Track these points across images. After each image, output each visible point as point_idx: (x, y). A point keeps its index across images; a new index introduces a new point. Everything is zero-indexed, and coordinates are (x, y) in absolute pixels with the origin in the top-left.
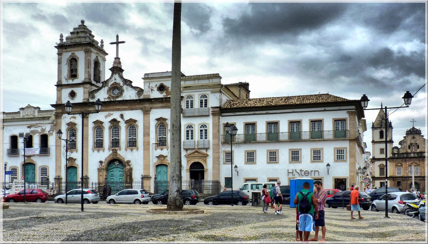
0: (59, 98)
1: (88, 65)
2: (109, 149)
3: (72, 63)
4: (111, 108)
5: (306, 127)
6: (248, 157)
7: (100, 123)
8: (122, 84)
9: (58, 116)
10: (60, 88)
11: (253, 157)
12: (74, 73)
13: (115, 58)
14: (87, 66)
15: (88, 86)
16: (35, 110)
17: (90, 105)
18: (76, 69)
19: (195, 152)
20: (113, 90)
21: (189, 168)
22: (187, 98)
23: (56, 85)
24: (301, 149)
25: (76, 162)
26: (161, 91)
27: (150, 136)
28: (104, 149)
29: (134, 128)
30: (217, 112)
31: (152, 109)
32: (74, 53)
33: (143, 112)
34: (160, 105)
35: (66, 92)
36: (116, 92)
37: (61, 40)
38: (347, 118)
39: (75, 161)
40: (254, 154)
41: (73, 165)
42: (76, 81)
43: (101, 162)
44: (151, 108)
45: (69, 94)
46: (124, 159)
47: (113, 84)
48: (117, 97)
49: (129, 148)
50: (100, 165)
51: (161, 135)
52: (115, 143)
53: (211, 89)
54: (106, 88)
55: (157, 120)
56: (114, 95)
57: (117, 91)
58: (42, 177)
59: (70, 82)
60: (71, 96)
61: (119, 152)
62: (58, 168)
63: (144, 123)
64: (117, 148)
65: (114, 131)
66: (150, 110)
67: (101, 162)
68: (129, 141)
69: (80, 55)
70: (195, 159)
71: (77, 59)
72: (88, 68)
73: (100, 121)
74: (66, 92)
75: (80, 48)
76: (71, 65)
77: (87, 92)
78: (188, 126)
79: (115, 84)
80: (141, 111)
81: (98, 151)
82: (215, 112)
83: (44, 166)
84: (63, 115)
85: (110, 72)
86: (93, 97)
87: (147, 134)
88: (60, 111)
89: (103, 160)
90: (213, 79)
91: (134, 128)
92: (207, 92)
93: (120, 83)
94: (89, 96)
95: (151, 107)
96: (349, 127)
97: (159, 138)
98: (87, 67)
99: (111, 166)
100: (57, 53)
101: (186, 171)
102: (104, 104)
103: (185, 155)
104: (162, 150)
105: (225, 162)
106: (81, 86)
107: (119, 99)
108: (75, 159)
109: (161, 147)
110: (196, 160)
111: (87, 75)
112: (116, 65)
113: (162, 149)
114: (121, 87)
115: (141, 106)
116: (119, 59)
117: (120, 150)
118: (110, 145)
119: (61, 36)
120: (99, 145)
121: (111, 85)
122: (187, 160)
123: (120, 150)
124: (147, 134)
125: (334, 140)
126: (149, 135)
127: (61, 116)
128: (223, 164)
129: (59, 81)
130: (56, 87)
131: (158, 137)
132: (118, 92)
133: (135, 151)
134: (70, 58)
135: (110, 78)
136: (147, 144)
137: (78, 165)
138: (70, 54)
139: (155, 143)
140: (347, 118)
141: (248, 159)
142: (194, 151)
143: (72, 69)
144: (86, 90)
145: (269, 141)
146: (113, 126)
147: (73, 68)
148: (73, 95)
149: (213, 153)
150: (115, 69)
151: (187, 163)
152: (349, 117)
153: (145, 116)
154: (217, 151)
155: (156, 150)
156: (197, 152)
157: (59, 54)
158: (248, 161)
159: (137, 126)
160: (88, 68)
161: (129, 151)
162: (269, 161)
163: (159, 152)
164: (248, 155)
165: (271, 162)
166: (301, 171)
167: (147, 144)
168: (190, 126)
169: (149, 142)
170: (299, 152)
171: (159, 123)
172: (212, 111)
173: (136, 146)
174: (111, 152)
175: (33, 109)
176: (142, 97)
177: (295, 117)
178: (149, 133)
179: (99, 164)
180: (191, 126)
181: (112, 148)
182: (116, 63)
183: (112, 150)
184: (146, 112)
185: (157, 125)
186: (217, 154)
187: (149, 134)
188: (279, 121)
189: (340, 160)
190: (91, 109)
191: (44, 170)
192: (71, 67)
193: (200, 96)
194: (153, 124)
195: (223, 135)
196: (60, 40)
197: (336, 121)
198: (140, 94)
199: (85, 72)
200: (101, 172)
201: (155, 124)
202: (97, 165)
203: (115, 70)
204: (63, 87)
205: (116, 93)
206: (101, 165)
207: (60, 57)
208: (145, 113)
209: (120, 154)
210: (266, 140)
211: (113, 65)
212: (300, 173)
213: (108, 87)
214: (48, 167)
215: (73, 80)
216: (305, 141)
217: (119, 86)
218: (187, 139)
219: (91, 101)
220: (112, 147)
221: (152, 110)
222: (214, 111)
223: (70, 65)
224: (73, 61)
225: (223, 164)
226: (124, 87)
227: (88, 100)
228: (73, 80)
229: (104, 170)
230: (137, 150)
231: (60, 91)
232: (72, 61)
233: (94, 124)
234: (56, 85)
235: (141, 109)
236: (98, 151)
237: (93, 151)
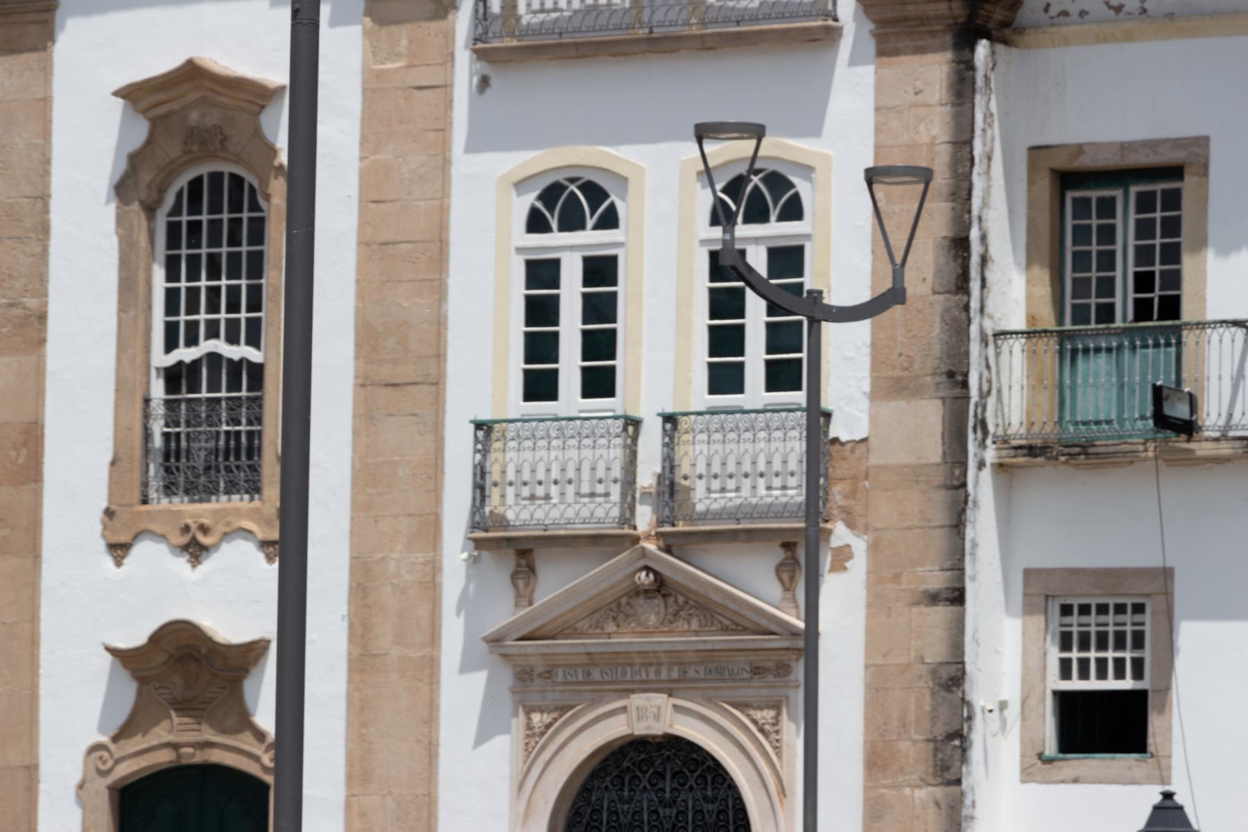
27: (42, 342)
51: (192, 327)
103: (495, 641)
104: (196, 560)
113: (195, 550)
128: (1027, 775)
131: (161, 359)
149: (877, 603)
156: (661, 587)
178: (31, 302)
180: (595, 193)
185: (146, 177)
186: (941, 613)
187: (42, 318)
195: (1029, 334)
218: (529, 395)
225: (1027, 775)
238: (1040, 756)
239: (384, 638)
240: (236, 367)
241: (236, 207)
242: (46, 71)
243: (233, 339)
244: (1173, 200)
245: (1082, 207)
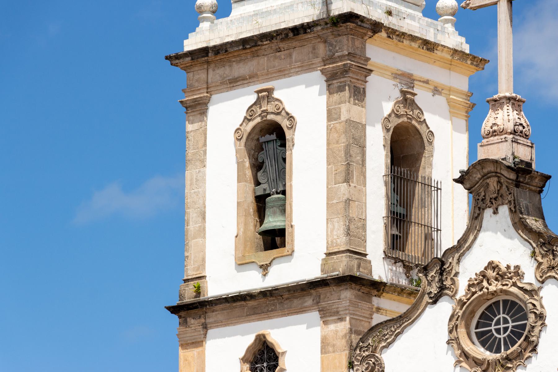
3: (262, 156)
20: (485, 319)
45: (244, 360)
56: (490, 349)
57: (506, 321)
71: (285, 124)
72: (347, 180)
77: (342, 343)
79: (491, 273)
93: (523, 269)
98: (341, 177)
106: (309, 301)
114: (532, 293)
130: (175, 318)
134: (252, 124)
143: (260, 192)
150: (485, 176)
192: (258, 183)
204: (212, 317)
205: (502, 336)
213: (452, 297)
215: (265, 268)
217: (514, 290)
223: (249, 173)
226: (542, 293)
231: (200, 349)
232: (263, 139)
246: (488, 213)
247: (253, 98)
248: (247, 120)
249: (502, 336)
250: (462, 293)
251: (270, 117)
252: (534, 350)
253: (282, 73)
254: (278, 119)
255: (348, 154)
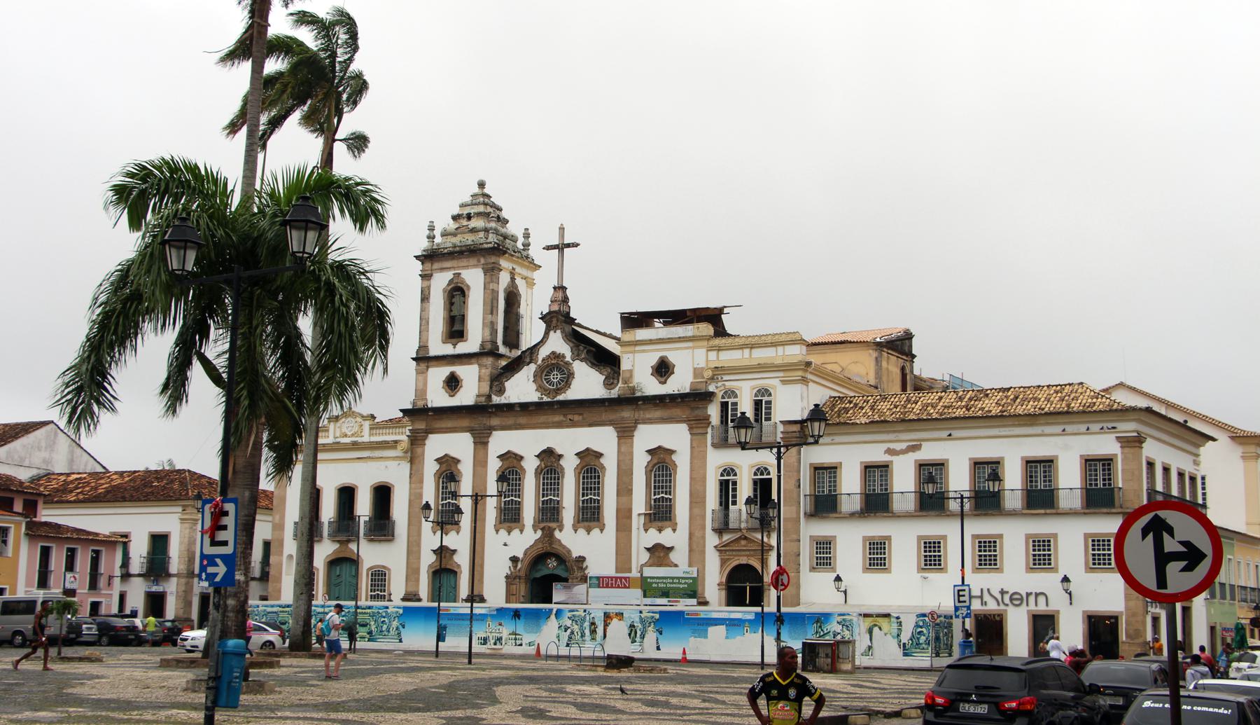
0: (421, 392)
1: (491, 308)
2: (535, 528)
3: (454, 300)
4: (542, 419)
5: (1013, 479)
6: (870, 554)
7: (515, 458)
8: (568, 358)
9: (417, 440)
10: (423, 366)
11: (885, 553)
12: (456, 328)
13: (555, 288)
14: (489, 308)
15: (489, 361)
16: (363, 423)
17: (492, 413)
18: (464, 316)
19: (740, 538)
20: (548, 374)
21: (724, 580)
22: (723, 397)
23: (413, 359)
24: (1001, 536)
25: (456, 558)
26: (661, 376)
28: (524, 525)
29: (595, 473)
30: (794, 434)
31: (640, 423)
32: (460, 274)
33: (618, 432)
34: (658, 413)
35: (439, 374)
36: (556, 377)
37: (431, 238)
38: (1116, 455)
39: (453, 554)
40: (886, 546)
41: (448, 567)
42: (463, 348)
43: (514, 560)
44: (637, 422)
46: (569, 551)
47: (549, 356)
48: (558, 391)
49: (582, 524)
50: (512, 568)
52: (549, 513)
53: (781, 374)
54: (533, 367)
55: (649, 452)
58: (373, 593)
59: (448, 349)
60: (448, 386)
61: (557, 534)
62: (412, 572)
63: (618, 460)
64: (553, 525)
65: (547, 479)
66: (636, 427)
67: (514, 560)
68: (583, 507)
69: (474, 277)
70: (741, 558)
71: (465, 288)
72: (492, 313)
73: (516, 455)
74: (439, 374)
75: (473, 261)
76: (452, 304)
77: (488, 378)
78: (725, 470)
79: (552, 356)
80: (468, 434)
81: (509, 533)
82: (789, 435)
83: (378, 566)
84: (430, 435)
85: (542, 326)
86: (501, 391)
87: (624, 489)
88: (421, 425)
89: (520, 556)
90: (786, 347)
91: (595, 473)
92: (772, 382)
94: (491, 388)
95: (636, 420)
96: (1122, 479)
97: (583, 501)
98: (489, 312)
99: (537, 571)
100: (420, 273)
101: (717, 587)
102: (525, 407)
105: (815, 566)
106: (473, 360)
107: (561, 397)
108: (454, 551)
109: (660, 524)
110: (743, 561)
111: (487, 332)
112: (555, 308)
113: (660, 530)
114: (568, 364)
115: (612, 416)
116: (563, 289)
117: (561, 531)
118: (537, 517)
119: (432, 228)
120: (510, 516)
121: (543, 360)
122: (722, 559)
123: (561, 531)
124: (624, 489)
125: (1085, 514)
126: (630, 492)
127: (425, 438)
128: (810, 571)
129: (423, 347)
131: (653, 497)
132: (559, 376)
133: (596, 531)
134: (450, 287)
135: (541, 341)
136: (624, 515)
137: (459, 566)
138: (449, 275)
139: (645, 514)
140: (1116, 455)
141: (870, 559)
142: (738, 535)
143: (452, 314)
144: (483, 371)
145: (920, 513)
146: (546, 467)
147: (455, 313)
148: (453, 383)
150: (552, 318)
151: (721, 566)
152: (1122, 453)
153: (622, 441)
154: (795, 537)
155: (646, 530)
156: (746, 538)
157: (426, 277)
158: (870, 565)
159: (603, 468)
160: (492, 313)
161: (582, 532)
162: (923, 566)
163: (653, 537)
164: (870, 549)
165: (928, 567)
166: (1003, 592)
167: (624, 515)
168: (729, 471)
169: (630, 510)
170: (998, 544)
171: (655, 461)
172: (782, 432)
173: (598, 520)
174: (539, 533)
175: (359, 419)
176: (614, 393)
177: (986, 449)
179: (510, 563)
180: (733, 470)
181: (542, 525)
182: (556, 301)
183: (543, 529)
184: (625, 433)
185: (651, 466)
187: (632, 490)
188: (947, 460)
189: (1102, 566)
190: (495, 421)
191: (380, 577)
192: (451, 311)
193: (755, 391)
194: (641, 461)
195: (810, 495)
196: (429, 237)
197: (1090, 463)
198: (612, 383)
199: (483, 323)
200: (514, 586)
201: (646, 464)
202: (505, 568)
203: (554, 321)
204: (431, 363)
205: (555, 380)
206: (515, 567)
207: (426, 283)
208: (620, 435)
209: (559, 541)
210: (915, 511)
211: (550, 305)
212: (999, 597)
214: (389, 570)
215: (455, 345)
216: (1013, 514)
219: (496, 400)
220: (543, 521)
221: (640, 426)
222: (788, 433)
223: (448, 306)
224: (457, 293)
225: (810, 571)
227: (489, 397)
228: (455, 345)
229: (522, 581)
230: (602, 530)
231: (424, 375)
233: (502, 460)
234: (413, 359)
235: (610, 423)
236: (509, 533)
237: (497, 531)
238: (814, 568)
239: (694, 547)
240: (666, 499)
241: (666, 471)
242: (632, 446)
243: (666, 494)
244: (835, 472)
245: (819, 473)
246: (552, 333)
247: (452, 276)
248: (448, 285)
249: (555, 380)
250: (540, 362)
251: (459, 285)
252: (569, 387)
253: (466, 267)
254: (462, 286)
255: (492, 303)
